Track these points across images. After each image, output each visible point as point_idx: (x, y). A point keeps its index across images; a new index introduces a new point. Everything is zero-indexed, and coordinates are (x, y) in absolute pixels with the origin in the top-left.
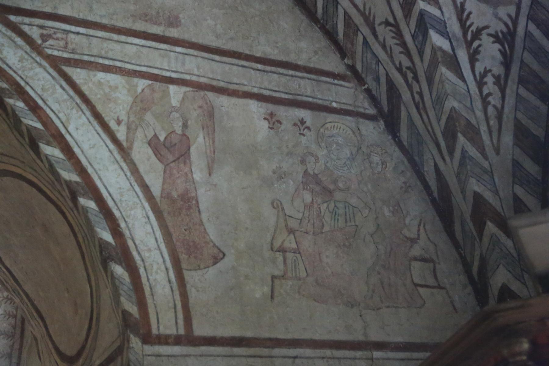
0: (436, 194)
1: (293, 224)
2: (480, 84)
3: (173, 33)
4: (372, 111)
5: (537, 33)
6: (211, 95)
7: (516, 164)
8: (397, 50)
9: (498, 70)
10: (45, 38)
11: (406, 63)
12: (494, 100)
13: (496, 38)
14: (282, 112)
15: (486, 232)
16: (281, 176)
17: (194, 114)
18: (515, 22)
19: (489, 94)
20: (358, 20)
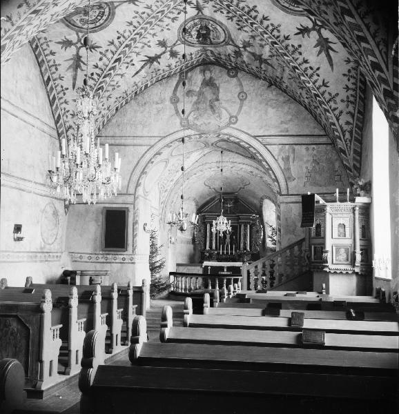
2: (346, 142)
3: (287, 134)
6: (294, 146)
9: (350, 138)
12: (349, 145)
14: (309, 146)
16: (308, 161)
17: (291, 150)
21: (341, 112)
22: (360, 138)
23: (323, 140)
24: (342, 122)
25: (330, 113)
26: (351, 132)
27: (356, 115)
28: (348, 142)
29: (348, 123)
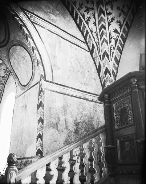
0: (98, 68)
1: (73, 67)
2: (111, 47)
4: (88, 50)
5: (121, 40)
7: (114, 64)
8: (96, 38)
9: (114, 45)
10: (31, 17)
11: (97, 41)
13: (115, 39)
15: (107, 75)
18: (118, 37)
19: (112, 50)
20: (89, 31)
21: (113, 19)
22: (121, 49)
23: (84, 46)
24: (112, 28)
25: (105, 16)
26: (116, 40)
27: (123, 26)
28: (112, 48)
29: (116, 31)
